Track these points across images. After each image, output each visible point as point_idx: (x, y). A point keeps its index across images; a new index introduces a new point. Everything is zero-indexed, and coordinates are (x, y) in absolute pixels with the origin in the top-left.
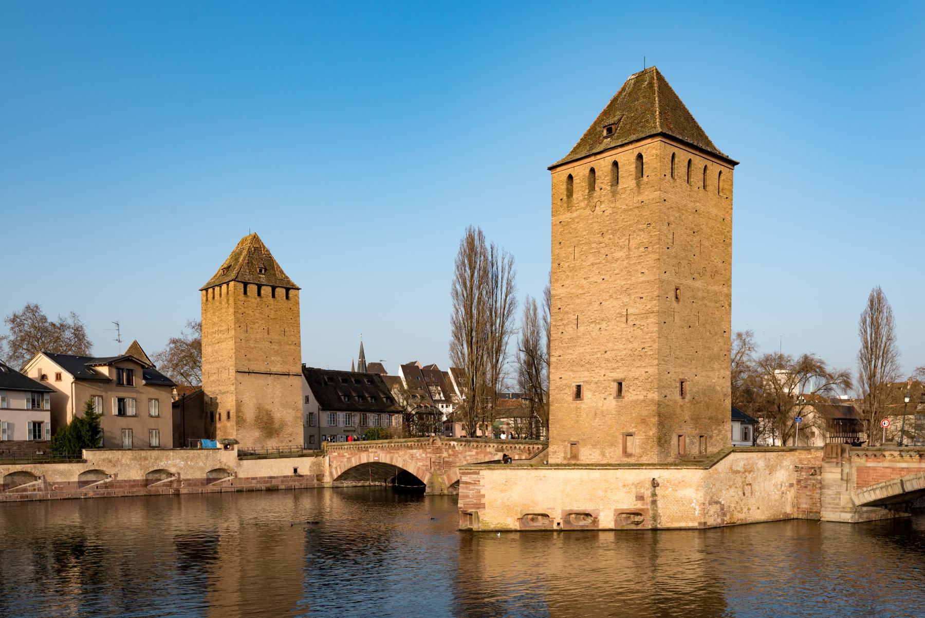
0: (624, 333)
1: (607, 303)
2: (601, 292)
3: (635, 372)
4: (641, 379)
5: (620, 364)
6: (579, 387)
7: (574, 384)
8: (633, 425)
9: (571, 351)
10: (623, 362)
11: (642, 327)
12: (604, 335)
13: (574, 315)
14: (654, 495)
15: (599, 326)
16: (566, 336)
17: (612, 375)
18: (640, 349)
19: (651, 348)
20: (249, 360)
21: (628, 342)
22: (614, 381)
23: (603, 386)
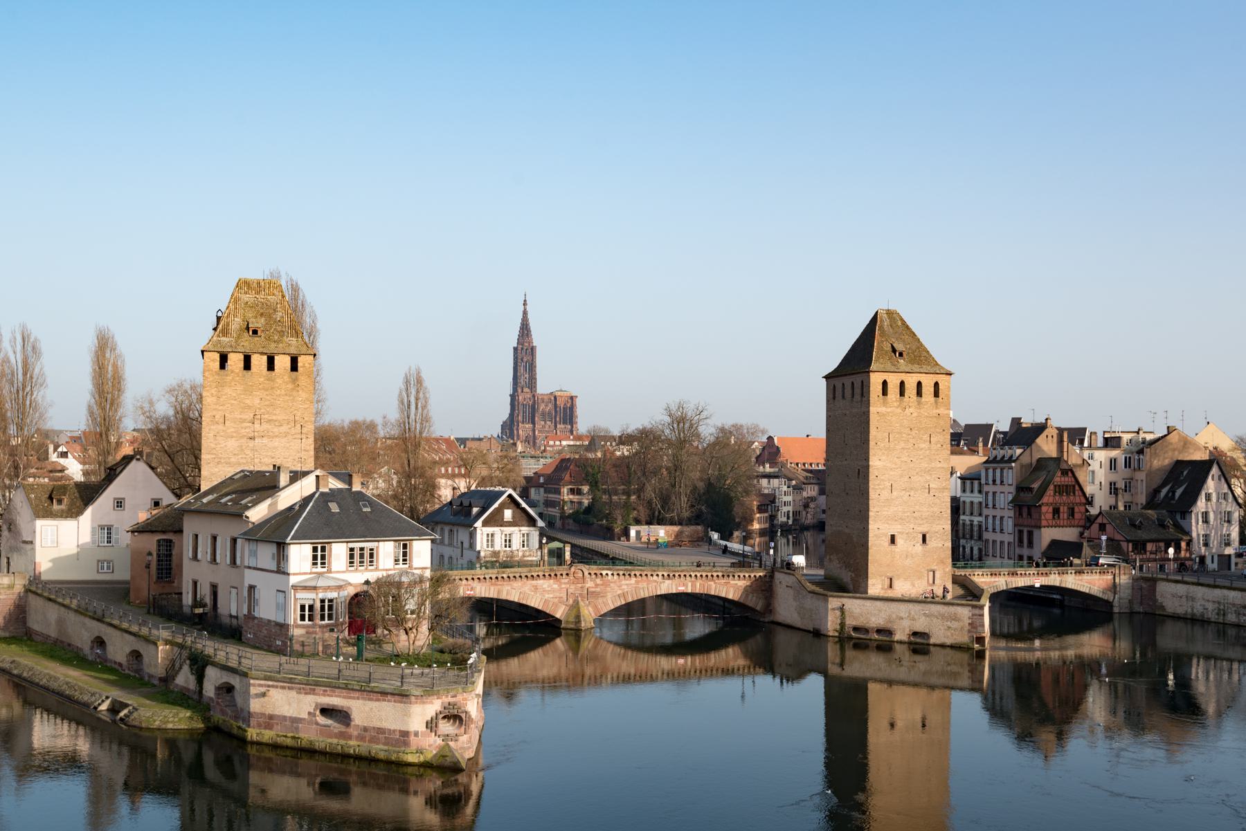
15: (908, 493)
16: (882, 498)
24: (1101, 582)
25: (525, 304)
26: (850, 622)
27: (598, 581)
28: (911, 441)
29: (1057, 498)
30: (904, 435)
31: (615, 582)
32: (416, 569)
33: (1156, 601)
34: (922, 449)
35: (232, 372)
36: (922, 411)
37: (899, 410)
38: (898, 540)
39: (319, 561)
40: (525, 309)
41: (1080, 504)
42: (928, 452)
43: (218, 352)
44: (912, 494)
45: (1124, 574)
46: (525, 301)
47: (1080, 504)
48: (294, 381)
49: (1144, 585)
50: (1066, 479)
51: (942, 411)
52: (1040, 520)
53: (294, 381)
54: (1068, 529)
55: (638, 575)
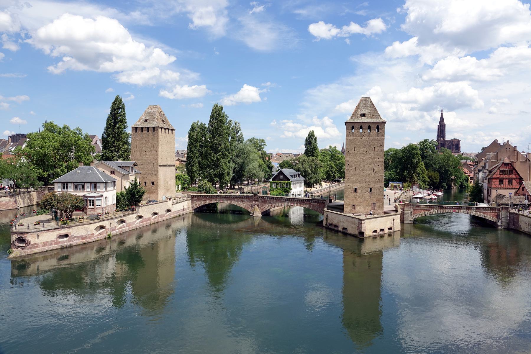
6: (356, 189)
7: (354, 188)
14: (393, 222)
16: (351, 173)
20: (162, 160)
22: (369, 188)
26: (329, 222)
27: (263, 200)
31: (268, 201)
32: (98, 192)
33: (519, 224)
35: (138, 133)
37: (360, 138)
38: (358, 190)
39: (65, 188)
40: (442, 112)
41: (516, 178)
43: (135, 127)
44: (365, 172)
46: (442, 110)
48: (154, 135)
49: (515, 216)
51: (380, 137)
52: (492, 185)
53: (154, 135)
55: (276, 199)
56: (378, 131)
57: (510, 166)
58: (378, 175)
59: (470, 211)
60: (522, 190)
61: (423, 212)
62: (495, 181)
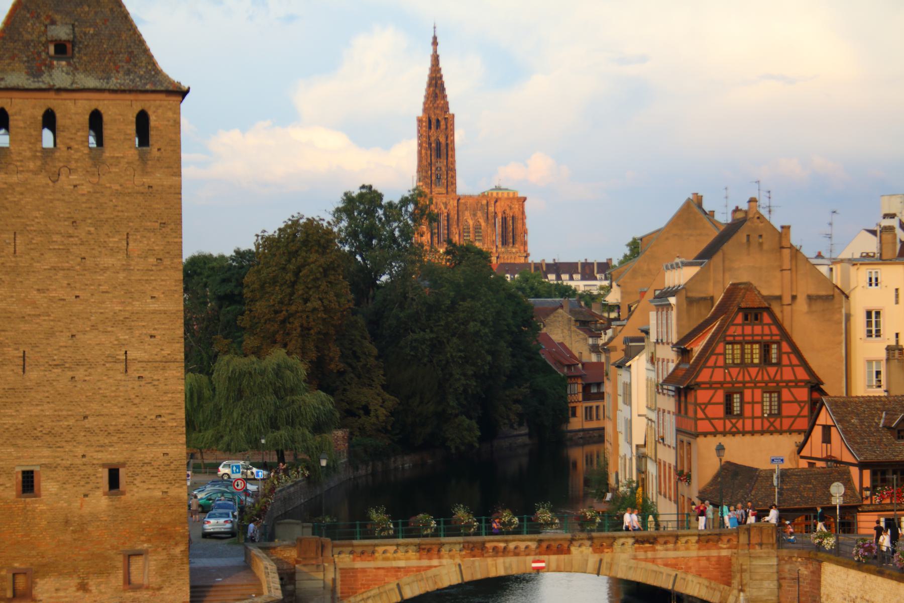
0: (121, 389)
1: (86, 337)
2: (74, 318)
3: (145, 453)
4: (156, 464)
5: (116, 438)
7: (19, 469)
8: (143, 538)
9: (9, 412)
10: (121, 436)
11: (156, 383)
12: (82, 389)
13: (17, 349)
15: (70, 374)
17: (100, 455)
18: (153, 417)
19: (174, 416)
21: (130, 404)
22: (104, 466)
23: (82, 473)
24: (703, 563)
25: (435, 43)
28: (74, 249)
29: (734, 371)
30: (56, 238)
34: (105, 269)
36: (104, 180)
37: (42, 179)
38: (47, 486)
40: (435, 51)
41: (797, 383)
42: (121, 276)
45: (761, 545)
46: (435, 38)
47: (797, 383)
49: (804, 571)
50: (758, 329)
51: (158, 178)
54: (767, 439)
56: (141, 144)
57: (769, 325)
58: (153, 390)
59: (607, 556)
60: (823, 442)
61: (393, 585)
62: (706, 400)
